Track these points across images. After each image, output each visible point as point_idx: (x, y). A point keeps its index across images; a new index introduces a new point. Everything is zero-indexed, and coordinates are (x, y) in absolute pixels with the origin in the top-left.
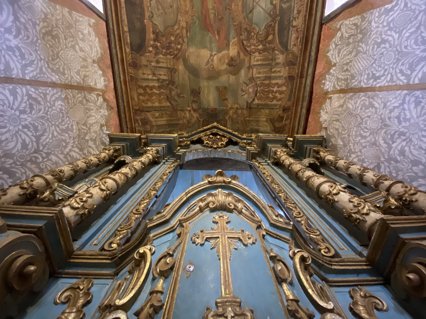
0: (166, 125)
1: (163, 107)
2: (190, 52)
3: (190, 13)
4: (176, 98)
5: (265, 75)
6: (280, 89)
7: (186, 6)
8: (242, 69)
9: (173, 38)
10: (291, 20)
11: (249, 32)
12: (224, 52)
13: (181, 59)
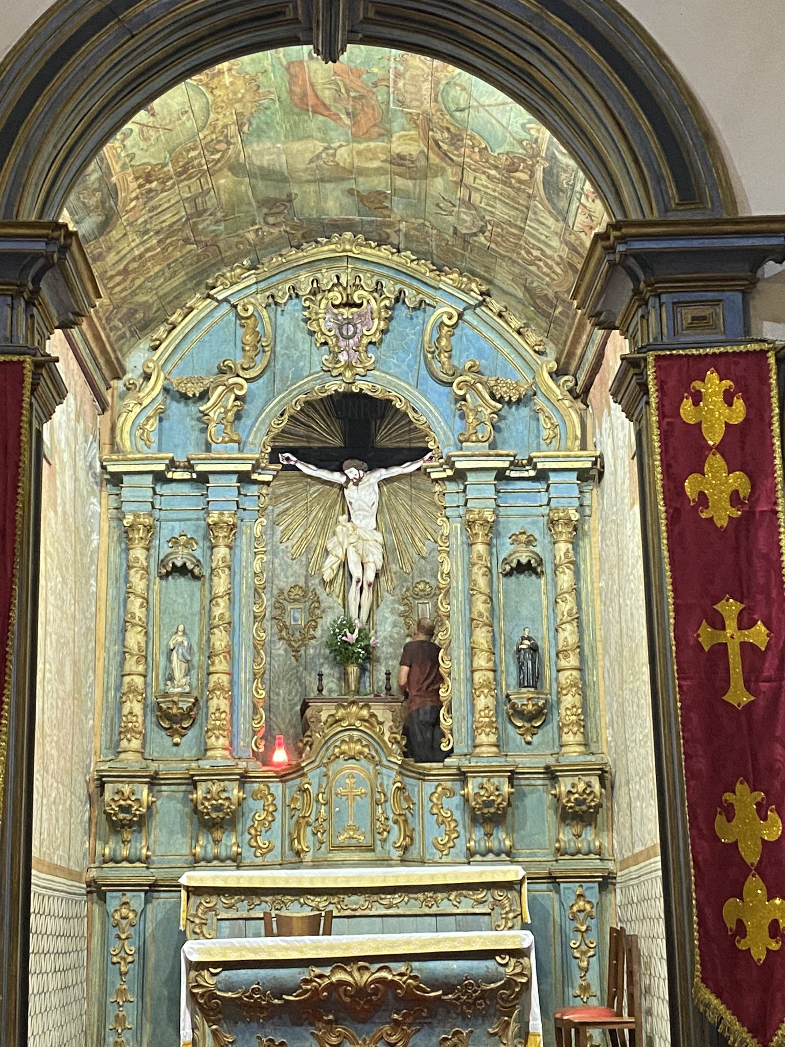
0: (184, 281)
1: (177, 260)
2: (253, 151)
3: (248, 97)
4: (213, 228)
5: (506, 217)
6: (549, 262)
7: (235, 93)
8: (436, 176)
9: (193, 154)
10: (578, 188)
11: (456, 139)
12: (372, 144)
13: (225, 170)
